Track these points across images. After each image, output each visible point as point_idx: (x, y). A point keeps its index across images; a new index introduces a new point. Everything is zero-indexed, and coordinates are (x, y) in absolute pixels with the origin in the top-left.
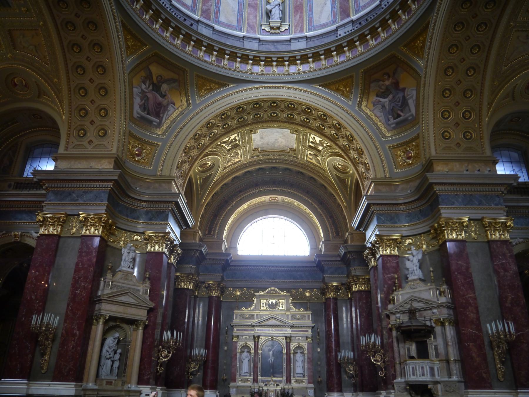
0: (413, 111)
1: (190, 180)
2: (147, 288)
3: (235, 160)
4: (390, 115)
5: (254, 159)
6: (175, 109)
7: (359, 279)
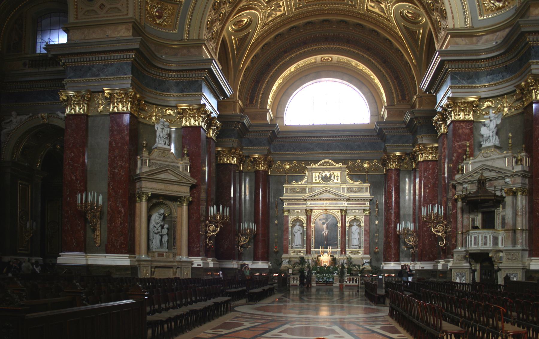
1: (224, 41)
3: (276, 14)
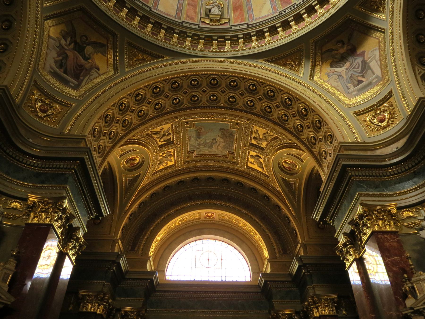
0: (378, 72)
2: (7, 272)
3: (167, 163)
4: (349, 83)
5: (189, 165)
6: (99, 75)
7: (321, 299)
